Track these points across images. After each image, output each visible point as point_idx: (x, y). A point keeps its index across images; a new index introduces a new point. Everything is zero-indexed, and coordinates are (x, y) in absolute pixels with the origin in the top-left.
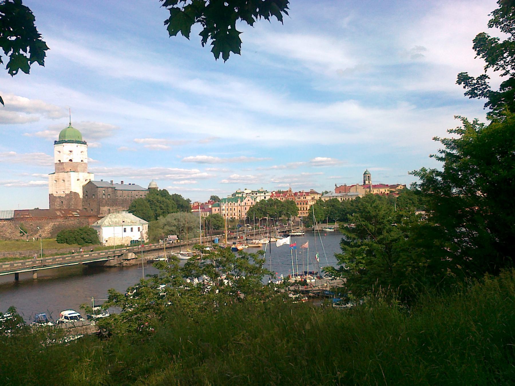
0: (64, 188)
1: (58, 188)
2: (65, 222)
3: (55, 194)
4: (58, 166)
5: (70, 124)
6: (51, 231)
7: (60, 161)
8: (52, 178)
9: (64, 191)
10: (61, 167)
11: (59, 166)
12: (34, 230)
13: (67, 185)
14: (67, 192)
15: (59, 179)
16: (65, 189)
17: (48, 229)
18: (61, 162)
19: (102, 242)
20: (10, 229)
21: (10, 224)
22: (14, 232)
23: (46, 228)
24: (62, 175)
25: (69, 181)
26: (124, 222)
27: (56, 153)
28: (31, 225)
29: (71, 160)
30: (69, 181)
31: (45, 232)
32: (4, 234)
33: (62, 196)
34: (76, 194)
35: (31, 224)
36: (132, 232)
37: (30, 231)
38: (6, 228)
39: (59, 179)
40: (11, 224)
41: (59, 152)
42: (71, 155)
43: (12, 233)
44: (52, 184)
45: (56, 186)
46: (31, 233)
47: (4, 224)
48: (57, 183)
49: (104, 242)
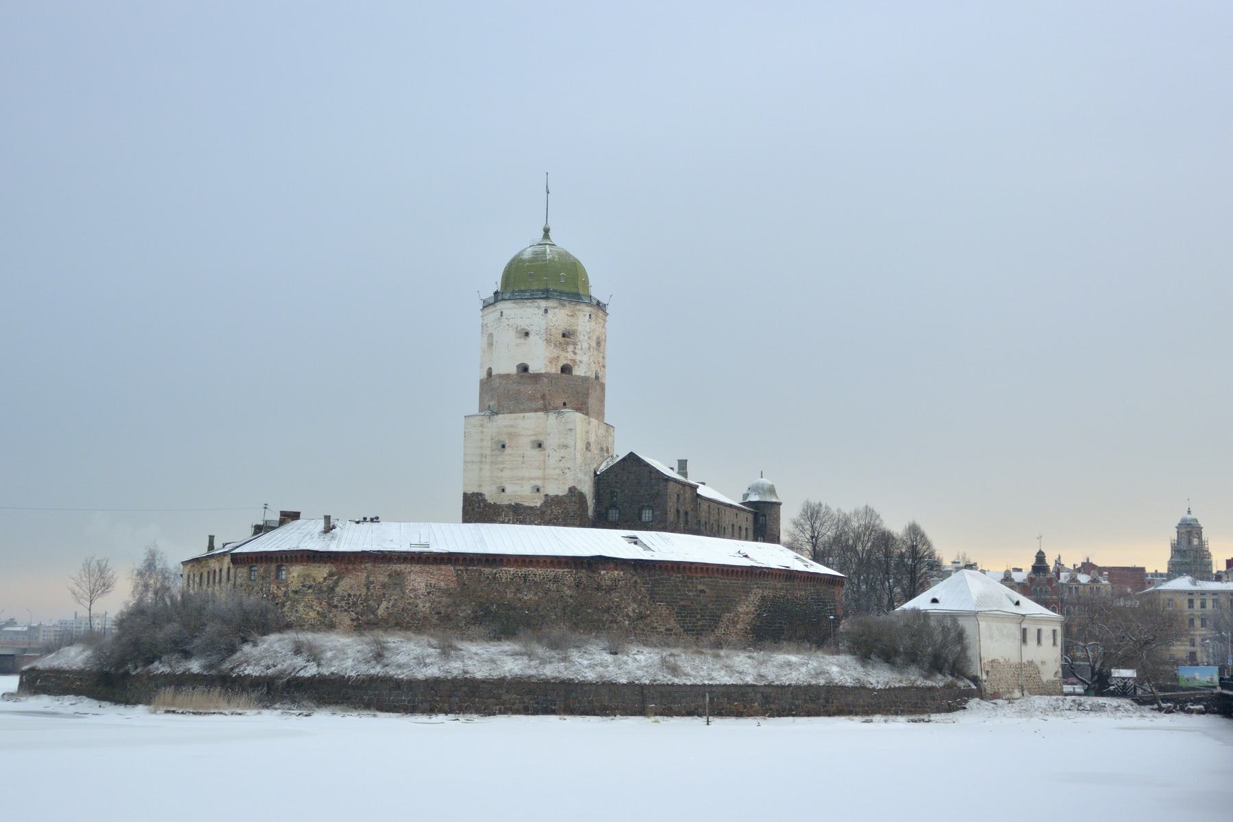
0: (539, 473)
1: (507, 474)
2: (787, 590)
3: (491, 495)
4: (515, 386)
5: (547, 231)
6: (754, 622)
7: (525, 368)
8: (482, 432)
9: (539, 483)
10: (528, 389)
11: (522, 388)
12: (708, 612)
13: (552, 461)
14: (557, 489)
16: (544, 478)
17: (747, 614)
18: (532, 370)
19: (979, 674)
20: (634, 600)
21: (636, 582)
22: (649, 616)
23: (740, 610)
24: (530, 423)
25: (566, 446)
26: (1017, 603)
28: (702, 591)
29: (566, 369)
30: (566, 446)
31: (737, 622)
32: (611, 622)
33: (526, 504)
34: (582, 497)
35: (700, 587)
36: (1041, 648)
37: (699, 616)
38: (622, 599)
40: (639, 581)
42: (570, 348)
43: (642, 617)
44: (482, 455)
45: (502, 463)
46: (700, 623)
47: (615, 580)
48: (508, 451)
49: (984, 677)
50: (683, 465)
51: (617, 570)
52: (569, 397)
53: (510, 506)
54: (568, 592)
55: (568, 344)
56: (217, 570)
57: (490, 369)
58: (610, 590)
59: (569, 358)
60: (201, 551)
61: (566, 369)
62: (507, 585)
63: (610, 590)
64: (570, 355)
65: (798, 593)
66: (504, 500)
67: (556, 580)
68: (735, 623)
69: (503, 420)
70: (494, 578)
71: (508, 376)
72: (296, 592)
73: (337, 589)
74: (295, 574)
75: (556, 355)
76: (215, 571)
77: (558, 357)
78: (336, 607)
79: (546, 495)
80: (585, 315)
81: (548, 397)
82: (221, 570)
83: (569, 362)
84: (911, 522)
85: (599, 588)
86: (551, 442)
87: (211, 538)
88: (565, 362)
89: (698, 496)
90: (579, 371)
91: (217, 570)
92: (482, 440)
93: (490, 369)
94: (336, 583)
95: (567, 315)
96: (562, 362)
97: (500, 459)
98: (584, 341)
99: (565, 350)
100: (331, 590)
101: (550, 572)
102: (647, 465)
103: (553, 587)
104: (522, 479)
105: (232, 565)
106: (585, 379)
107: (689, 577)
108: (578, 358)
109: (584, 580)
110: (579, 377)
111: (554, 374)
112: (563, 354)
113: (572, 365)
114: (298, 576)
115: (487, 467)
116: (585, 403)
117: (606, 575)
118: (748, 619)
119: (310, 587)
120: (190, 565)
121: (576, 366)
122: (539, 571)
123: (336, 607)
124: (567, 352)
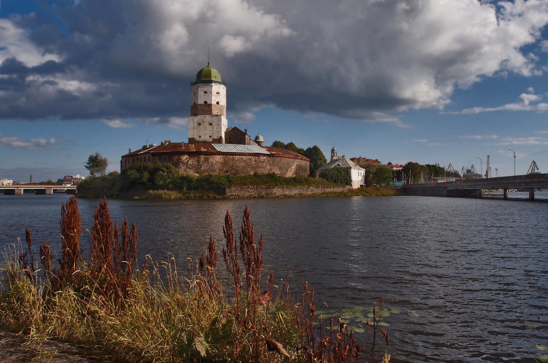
1: (201, 132)
3: (197, 138)
5: (208, 63)
7: (206, 102)
8: (194, 120)
11: (205, 108)
15: (203, 122)
24: (208, 118)
27: (201, 93)
28: (284, 163)
29: (218, 103)
33: (208, 141)
35: (284, 161)
39: (203, 122)
41: (206, 92)
42: (219, 97)
45: (200, 129)
48: (202, 126)
50: (246, 130)
51: (264, 156)
53: (202, 142)
54: (253, 163)
55: (218, 96)
56: (143, 158)
57: (195, 102)
58: (263, 162)
60: (127, 153)
61: (218, 103)
62: (237, 161)
63: (263, 162)
64: (219, 99)
65: (303, 163)
66: (201, 139)
67: (250, 159)
68: (291, 171)
69: (199, 117)
70: (234, 159)
71: (201, 104)
72: (176, 163)
73: (189, 163)
74: (176, 158)
76: (141, 158)
78: (188, 167)
79: (213, 138)
81: (213, 111)
82: (145, 158)
84: (314, 145)
85: (260, 162)
86: (214, 124)
87: (130, 150)
89: (250, 139)
91: (143, 158)
92: (194, 123)
93: (195, 102)
94: (188, 161)
97: (199, 128)
99: (217, 97)
100: (187, 162)
101: (249, 157)
102: (240, 130)
103: (249, 161)
104: (206, 133)
105: (151, 156)
106: (222, 106)
107: (282, 159)
109: (257, 160)
110: (221, 105)
114: (177, 159)
115: (195, 130)
116: (223, 113)
117: (262, 158)
118: (293, 170)
119: (181, 162)
120: (126, 158)
122: (245, 157)
123: (188, 167)
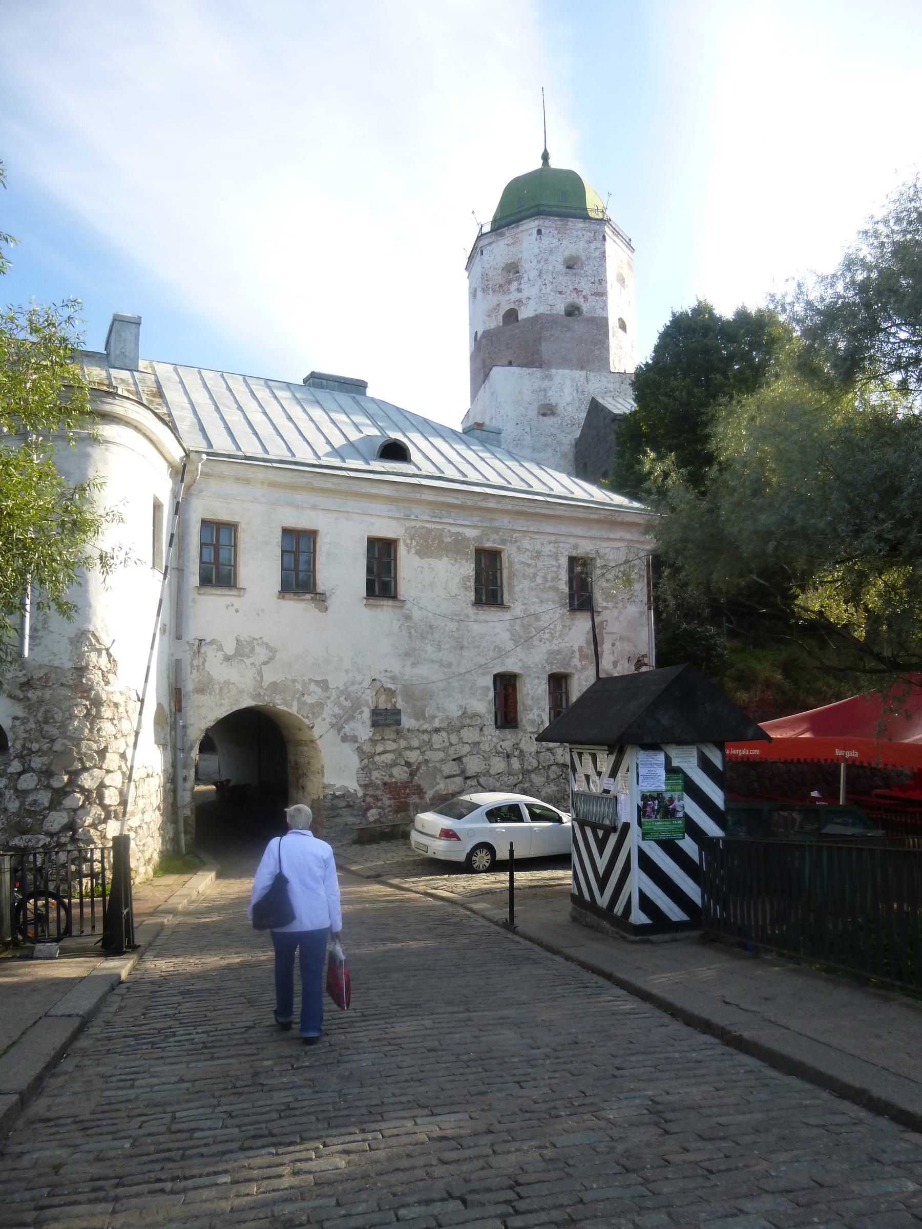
29: (511, 316)
52: (515, 352)
59: (513, 299)
61: (511, 316)
64: (515, 296)
75: (495, 303)
77: (498, 305)
80: (530, 235)
83: (512, 306)
88: (507, 308)
90: (525, 313)
95: (508, 245)
96: (505, 308)
98: (529, 269)
108: (524, 294)
111: (494, 329)
112: (507, 297)
113: (517, 308)
121: (522, 307)
124: (510, 293)
